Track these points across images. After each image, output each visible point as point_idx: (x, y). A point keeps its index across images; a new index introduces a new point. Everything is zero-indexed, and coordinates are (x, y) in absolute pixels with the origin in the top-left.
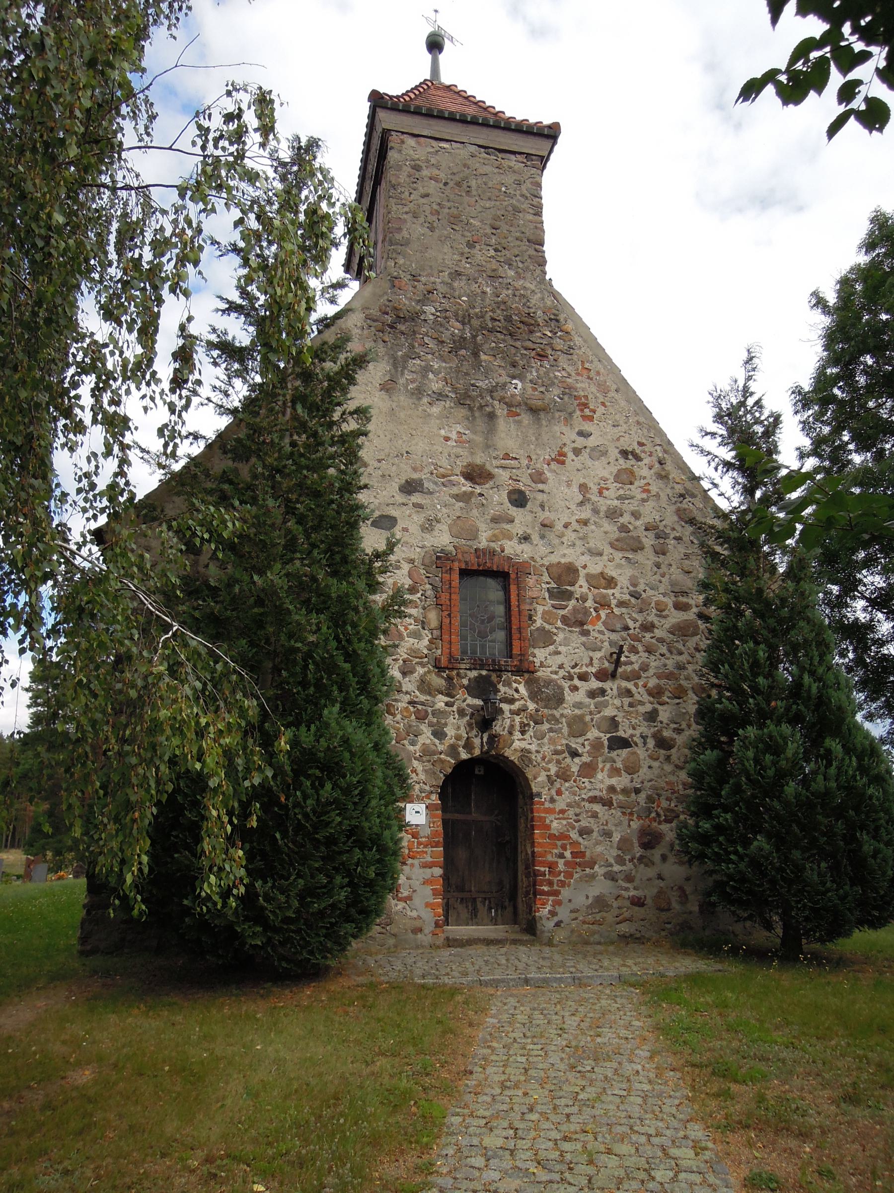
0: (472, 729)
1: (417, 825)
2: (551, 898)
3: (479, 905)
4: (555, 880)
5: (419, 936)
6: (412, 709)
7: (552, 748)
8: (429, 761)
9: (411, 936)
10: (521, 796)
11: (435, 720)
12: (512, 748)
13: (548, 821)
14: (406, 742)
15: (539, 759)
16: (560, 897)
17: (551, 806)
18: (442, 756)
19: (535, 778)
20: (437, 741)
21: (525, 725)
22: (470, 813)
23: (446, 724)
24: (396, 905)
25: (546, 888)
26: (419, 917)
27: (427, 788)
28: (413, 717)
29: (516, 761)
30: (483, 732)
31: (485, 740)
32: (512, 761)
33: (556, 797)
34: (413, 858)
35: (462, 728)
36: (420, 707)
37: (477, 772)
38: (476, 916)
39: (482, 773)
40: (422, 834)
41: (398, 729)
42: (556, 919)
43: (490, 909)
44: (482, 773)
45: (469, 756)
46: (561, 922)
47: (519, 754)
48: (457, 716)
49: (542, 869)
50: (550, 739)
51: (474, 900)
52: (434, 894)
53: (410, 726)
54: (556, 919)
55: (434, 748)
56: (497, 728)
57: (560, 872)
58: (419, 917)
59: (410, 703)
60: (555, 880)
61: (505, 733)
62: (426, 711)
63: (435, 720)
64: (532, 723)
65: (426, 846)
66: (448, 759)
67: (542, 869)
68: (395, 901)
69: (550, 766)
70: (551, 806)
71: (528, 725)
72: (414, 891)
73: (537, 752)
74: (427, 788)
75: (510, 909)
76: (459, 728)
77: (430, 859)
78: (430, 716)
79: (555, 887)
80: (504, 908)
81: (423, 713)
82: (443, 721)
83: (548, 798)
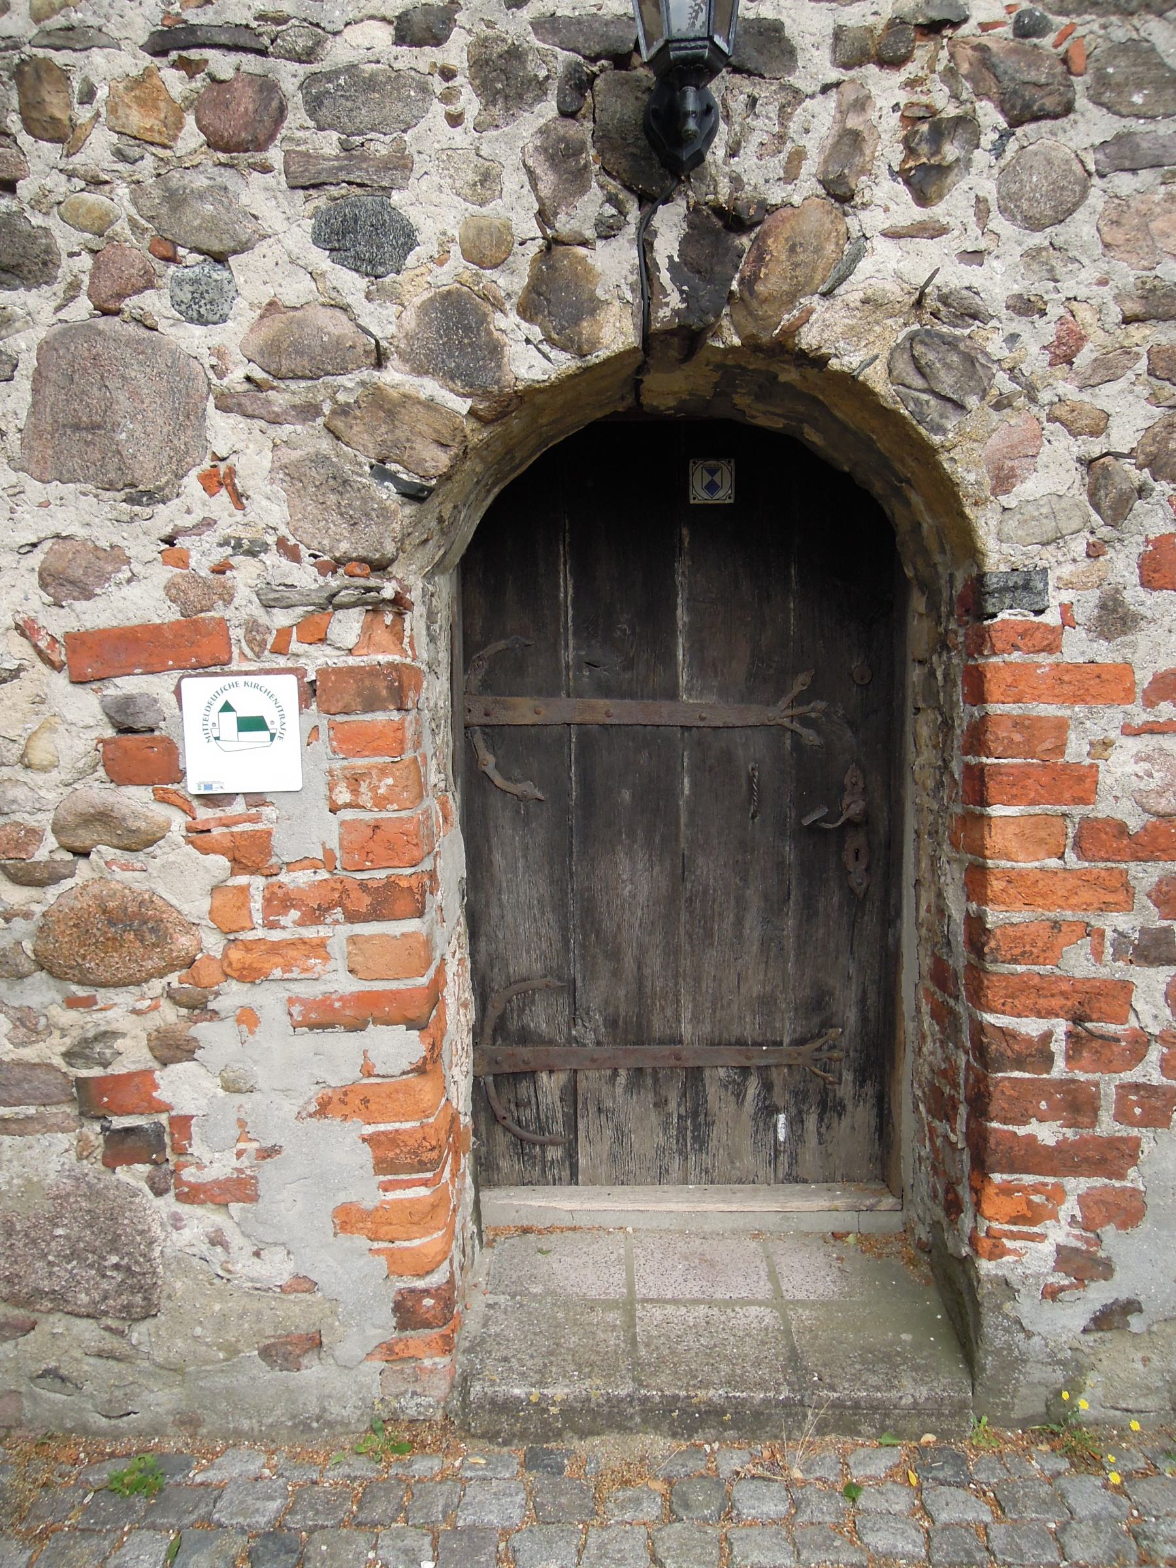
0: (576, 180)
1: (257, 799)
2: (1076, 1185)
3: (714, 1094)
4: (1109, 1084)
5: (313, 1372)
6: (175, 82)
7: (1126, 274)
8: (308, 411)
9: (266, 1374)
10: (918, 603)
11: (328, 143)
12: (852, 291)
13: (1076, 750)
14: (155, 303)
15: (1034, 360)
16: (1133, 1178)
17: (1104, 652)
18: (394, 376)
19: (1003, 481)
20: (352, 284)
21: (941, 130)
22: (671, 694)
23: (401, 164)
24: (177, 1222)
25: (1047, 1133)
26: (303, 1284)
27: (305, 577)
28: (191, 137)
29: (877, 380)
30: (649, 201)
31: (667, 246)
32: (851, 385)
33: (1135, 596)
34: (250, 975)
35: (513, 181)
36: (222, 64)
37: (699, 495)
38: (701, 1142)
39: (725, 495)
40: (285, 847)
41: (101, 227)
42: (1099, 1295)
43: (768, 1111)
44: (725, 495)
45: (564, 363)
46: (1131, 1307)
47: (896, 331)
48: (469, 102)
49: (1031, 1027)
50: (1120, 206)
51: (695, 1075)
52: (382, 1166)
53: (176, 199)
54: (1099, 1295)
55: (336, 325)
56: (747, 164)
57: (1139, 1044)
58: (303, 1284)
59: (159, 45)
60: (1109, 1084)
61: (807, 187)
62: (267, 87)
63: (328, 143)
64: (990, 115)
65: (315, 915)
66: (430, 387)
67: (1031, 1027)
68: (167, 1204)
69: (1108, 397)
70: (1104, 652)
71: (966, 123)
72: (268, 1153)
73: (1026, 307)
74: (305, 577)
75: (861, 1115)
76: (487, 179)
77: (348, 985)
78: (297, 116)
79: (1107, 1126)
80: (830, 1107)
81: (246, 101)
82: (381, 146)
83: (1086, 605)
